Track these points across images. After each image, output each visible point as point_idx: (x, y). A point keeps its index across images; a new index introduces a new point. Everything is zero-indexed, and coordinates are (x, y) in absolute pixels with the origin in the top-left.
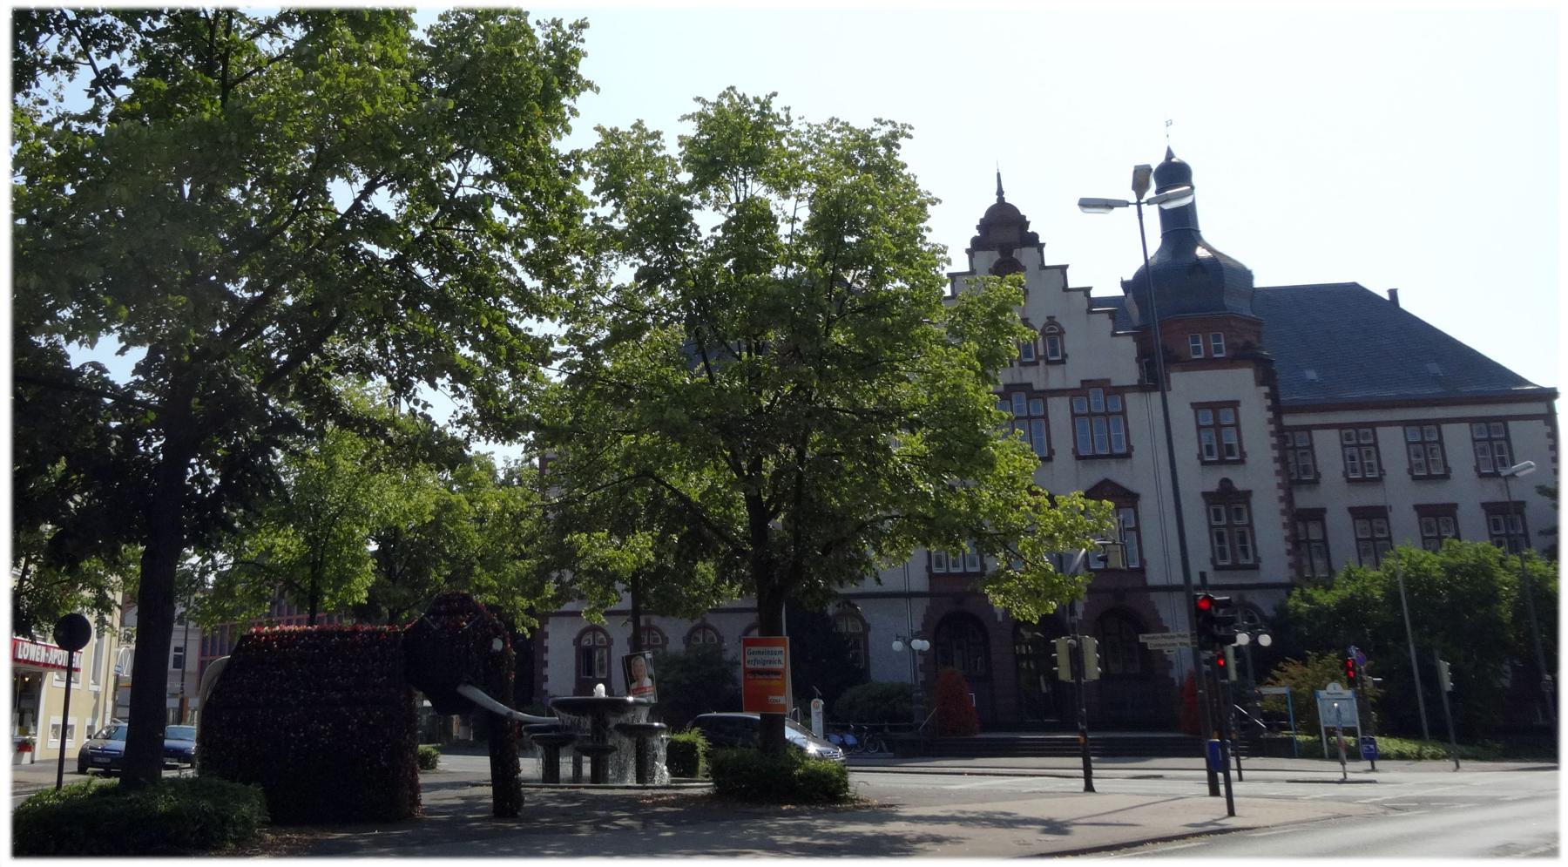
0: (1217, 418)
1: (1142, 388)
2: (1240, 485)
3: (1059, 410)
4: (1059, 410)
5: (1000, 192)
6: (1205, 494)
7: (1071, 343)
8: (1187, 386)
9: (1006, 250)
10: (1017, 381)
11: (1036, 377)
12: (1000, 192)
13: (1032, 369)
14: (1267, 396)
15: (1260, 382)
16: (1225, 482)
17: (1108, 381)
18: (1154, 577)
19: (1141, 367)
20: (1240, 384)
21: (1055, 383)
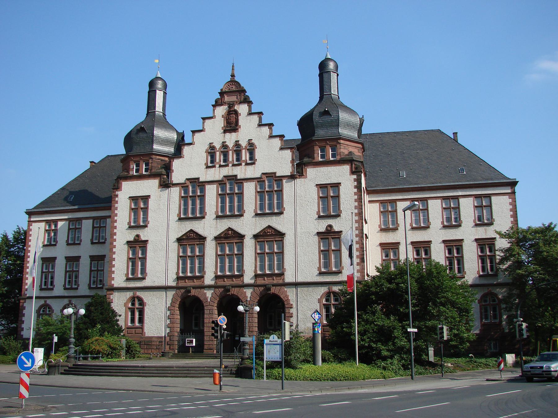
0: (329, 193)
1: (292, 177)
2: (336, 228)
3: (250, 189)
4: (250, 189)
5: (233, 76)
6: (318, 234)
7: (258, 154)
8: (316, 175)
9: (231, 105)
10: (230, 174)
11: (241, 172)
12: (233, 76)
13: (239, 167)
14: (355, 180)
15: (352, 173)
16: (330, 226)
17: (275, 173)
18: (289, 278)
19: (293, 165)
20: (341, 175)
21: (248, 176)
